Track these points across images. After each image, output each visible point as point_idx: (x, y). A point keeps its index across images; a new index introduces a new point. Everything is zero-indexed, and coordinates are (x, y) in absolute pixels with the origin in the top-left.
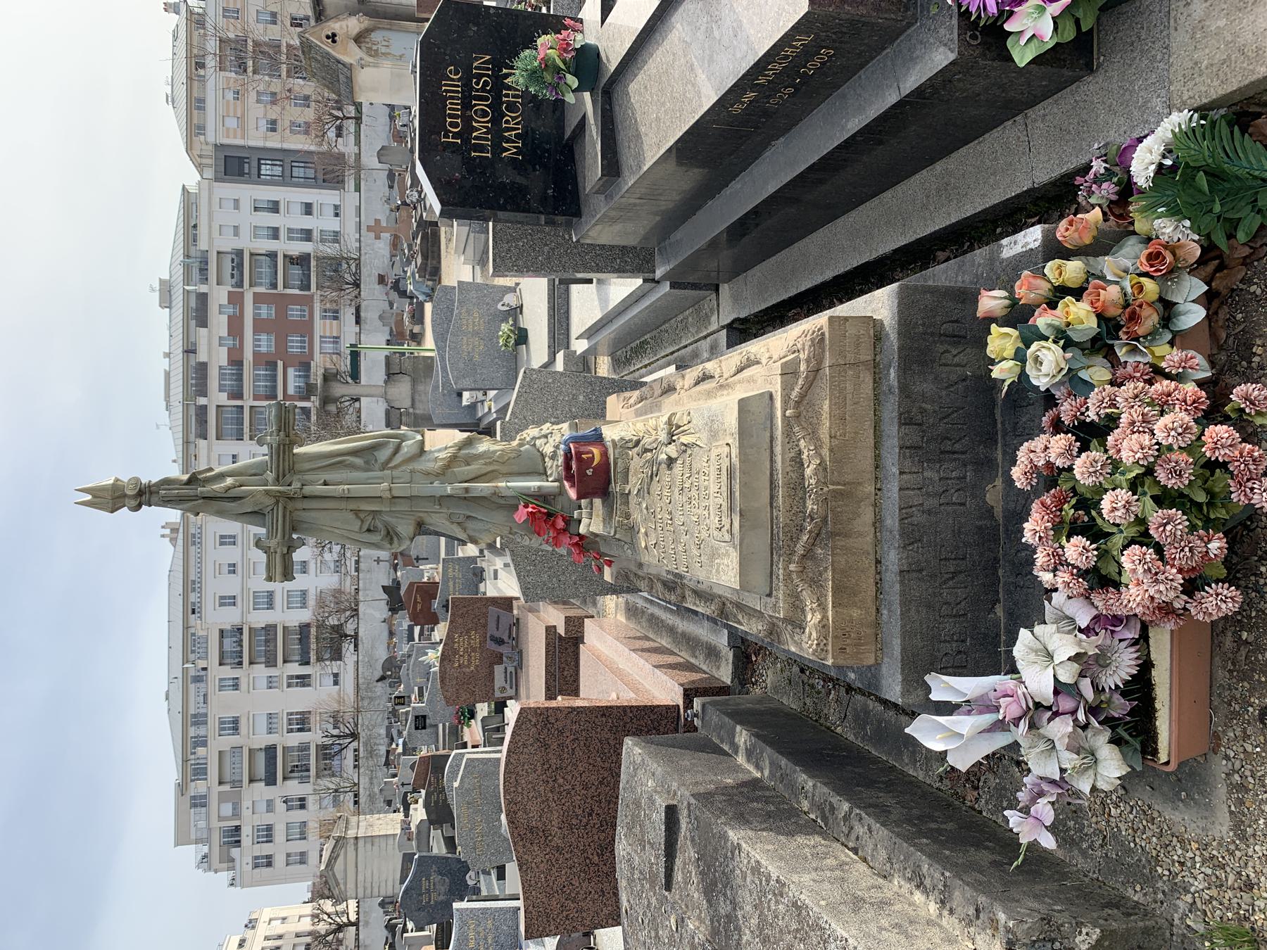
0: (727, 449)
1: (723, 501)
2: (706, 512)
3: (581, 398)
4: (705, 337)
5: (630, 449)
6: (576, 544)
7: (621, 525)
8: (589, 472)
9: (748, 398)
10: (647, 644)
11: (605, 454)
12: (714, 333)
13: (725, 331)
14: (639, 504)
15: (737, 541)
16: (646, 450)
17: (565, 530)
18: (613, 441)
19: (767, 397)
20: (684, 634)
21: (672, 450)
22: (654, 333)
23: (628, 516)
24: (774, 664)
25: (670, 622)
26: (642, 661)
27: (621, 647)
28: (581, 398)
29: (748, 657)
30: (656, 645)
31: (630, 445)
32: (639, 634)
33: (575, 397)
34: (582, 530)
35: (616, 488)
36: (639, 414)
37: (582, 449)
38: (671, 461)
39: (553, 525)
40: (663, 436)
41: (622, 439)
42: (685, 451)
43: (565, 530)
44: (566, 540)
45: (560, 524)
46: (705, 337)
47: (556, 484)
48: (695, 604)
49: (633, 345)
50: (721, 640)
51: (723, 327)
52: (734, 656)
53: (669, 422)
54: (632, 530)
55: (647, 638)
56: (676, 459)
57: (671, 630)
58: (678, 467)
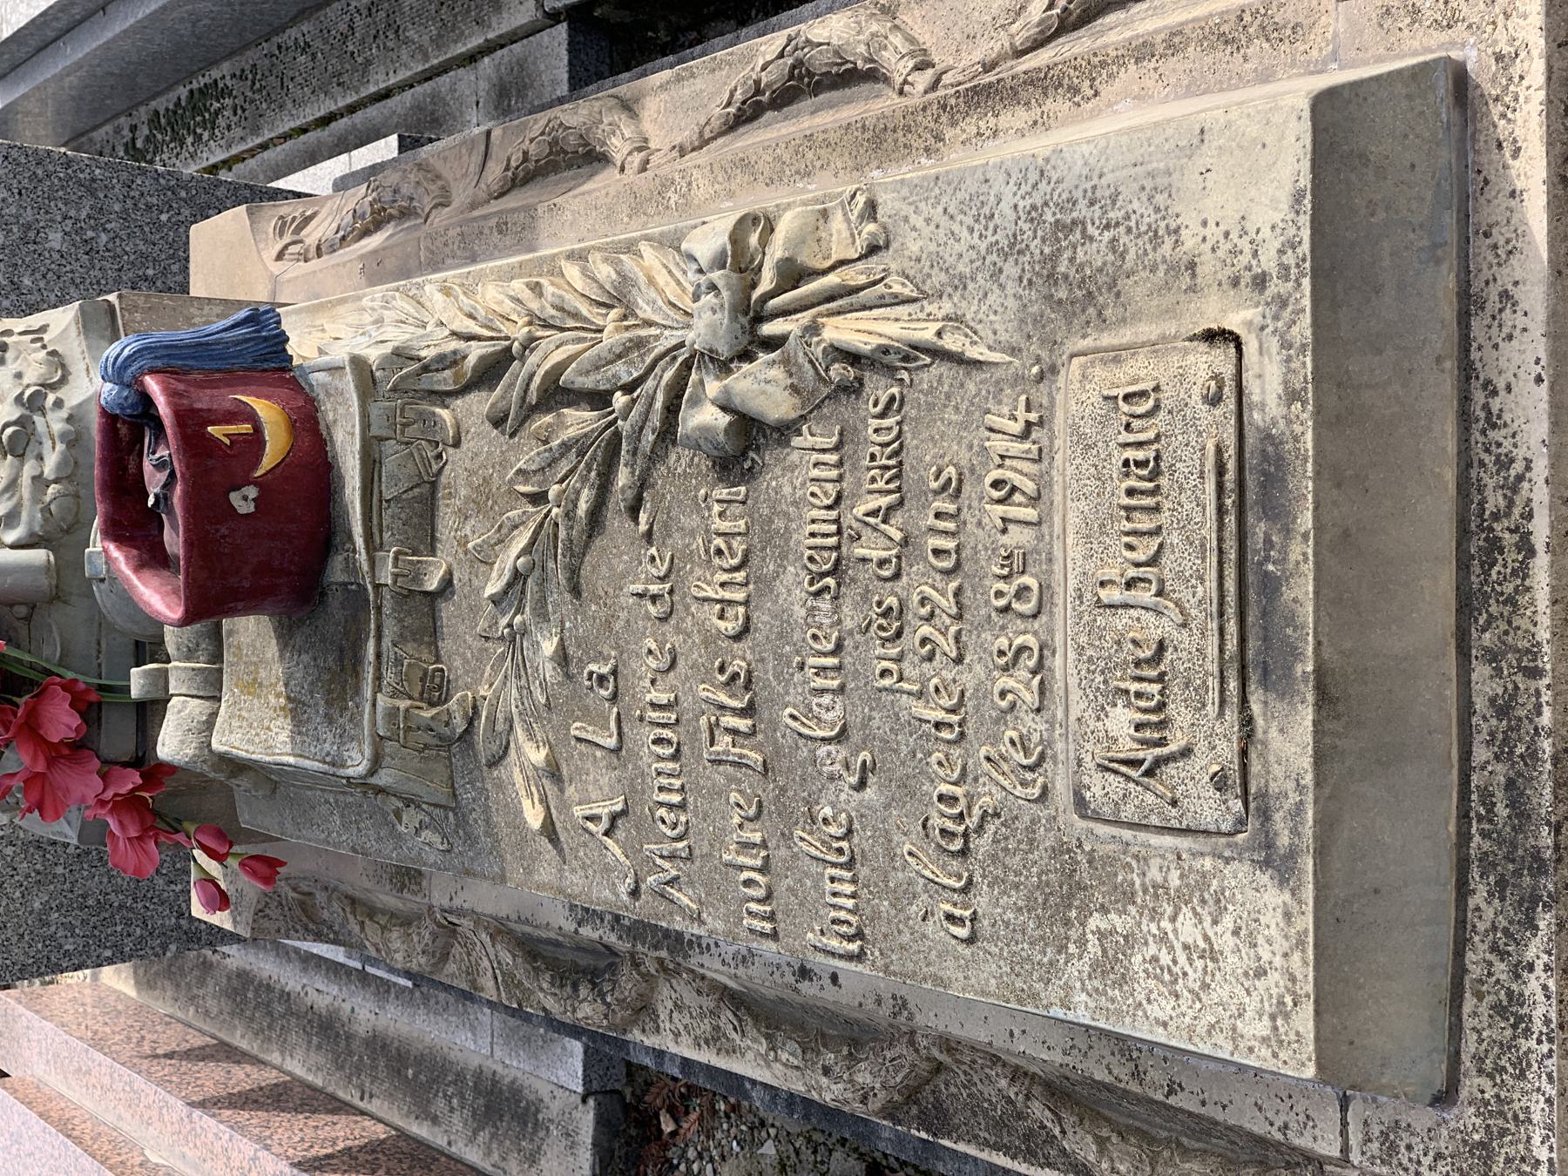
0: (1210, 362)
1: (1187, 622)
2: (1020, 683)
3: (55, 239)
4: (472, 58)
5: (443, 397)
6: (129, 804)
7: (401, 728)
8: (243, 501)
9: (1355, 86)
10: (243, 1077)
11: (308, 424)
12: (513, 38)
13: (562, 31)
14: (514, 638)
15: (1295, 828)
16: (556, 394)
17: (77, 749)
18: (358, 363)
19: (1443, 85)
20: (378, 1045)
21: (763, 386)
22: (252, 55)
23: (435, 689)
24: (750, 1142)
25: (322, 1003)
26: (247, 1147)
27: (150, 1092)
28: (55, 239)
29: (648, 1123)
30: (270, 1077)
31: (445, 380)
32: (197, 1041)
33: (31, 236)
34: (171, 744)
35: (368, 560)
36: (377, 271)
37: (203, 400)
38: (748, 444)
39: (31, 730)
40: (708, 325)
41: (401, 355)
42: (852, 389)
43: (77, 749)
44: (84, 785)
45: (62, 721)
46: (472, 58)
47: (39, 556)
48: (715, 1039)
49: (162, 104)
50: (562, 1073)
51: (554, 17)
52: (602, 1121)
53: (739, 259)
54: (456, 751)
55: (226, 1053)
56: (785, 431)
57: (327, 1030)
58: (800, 473)
